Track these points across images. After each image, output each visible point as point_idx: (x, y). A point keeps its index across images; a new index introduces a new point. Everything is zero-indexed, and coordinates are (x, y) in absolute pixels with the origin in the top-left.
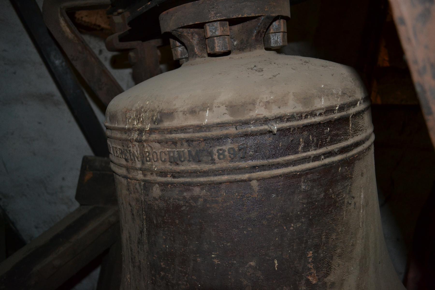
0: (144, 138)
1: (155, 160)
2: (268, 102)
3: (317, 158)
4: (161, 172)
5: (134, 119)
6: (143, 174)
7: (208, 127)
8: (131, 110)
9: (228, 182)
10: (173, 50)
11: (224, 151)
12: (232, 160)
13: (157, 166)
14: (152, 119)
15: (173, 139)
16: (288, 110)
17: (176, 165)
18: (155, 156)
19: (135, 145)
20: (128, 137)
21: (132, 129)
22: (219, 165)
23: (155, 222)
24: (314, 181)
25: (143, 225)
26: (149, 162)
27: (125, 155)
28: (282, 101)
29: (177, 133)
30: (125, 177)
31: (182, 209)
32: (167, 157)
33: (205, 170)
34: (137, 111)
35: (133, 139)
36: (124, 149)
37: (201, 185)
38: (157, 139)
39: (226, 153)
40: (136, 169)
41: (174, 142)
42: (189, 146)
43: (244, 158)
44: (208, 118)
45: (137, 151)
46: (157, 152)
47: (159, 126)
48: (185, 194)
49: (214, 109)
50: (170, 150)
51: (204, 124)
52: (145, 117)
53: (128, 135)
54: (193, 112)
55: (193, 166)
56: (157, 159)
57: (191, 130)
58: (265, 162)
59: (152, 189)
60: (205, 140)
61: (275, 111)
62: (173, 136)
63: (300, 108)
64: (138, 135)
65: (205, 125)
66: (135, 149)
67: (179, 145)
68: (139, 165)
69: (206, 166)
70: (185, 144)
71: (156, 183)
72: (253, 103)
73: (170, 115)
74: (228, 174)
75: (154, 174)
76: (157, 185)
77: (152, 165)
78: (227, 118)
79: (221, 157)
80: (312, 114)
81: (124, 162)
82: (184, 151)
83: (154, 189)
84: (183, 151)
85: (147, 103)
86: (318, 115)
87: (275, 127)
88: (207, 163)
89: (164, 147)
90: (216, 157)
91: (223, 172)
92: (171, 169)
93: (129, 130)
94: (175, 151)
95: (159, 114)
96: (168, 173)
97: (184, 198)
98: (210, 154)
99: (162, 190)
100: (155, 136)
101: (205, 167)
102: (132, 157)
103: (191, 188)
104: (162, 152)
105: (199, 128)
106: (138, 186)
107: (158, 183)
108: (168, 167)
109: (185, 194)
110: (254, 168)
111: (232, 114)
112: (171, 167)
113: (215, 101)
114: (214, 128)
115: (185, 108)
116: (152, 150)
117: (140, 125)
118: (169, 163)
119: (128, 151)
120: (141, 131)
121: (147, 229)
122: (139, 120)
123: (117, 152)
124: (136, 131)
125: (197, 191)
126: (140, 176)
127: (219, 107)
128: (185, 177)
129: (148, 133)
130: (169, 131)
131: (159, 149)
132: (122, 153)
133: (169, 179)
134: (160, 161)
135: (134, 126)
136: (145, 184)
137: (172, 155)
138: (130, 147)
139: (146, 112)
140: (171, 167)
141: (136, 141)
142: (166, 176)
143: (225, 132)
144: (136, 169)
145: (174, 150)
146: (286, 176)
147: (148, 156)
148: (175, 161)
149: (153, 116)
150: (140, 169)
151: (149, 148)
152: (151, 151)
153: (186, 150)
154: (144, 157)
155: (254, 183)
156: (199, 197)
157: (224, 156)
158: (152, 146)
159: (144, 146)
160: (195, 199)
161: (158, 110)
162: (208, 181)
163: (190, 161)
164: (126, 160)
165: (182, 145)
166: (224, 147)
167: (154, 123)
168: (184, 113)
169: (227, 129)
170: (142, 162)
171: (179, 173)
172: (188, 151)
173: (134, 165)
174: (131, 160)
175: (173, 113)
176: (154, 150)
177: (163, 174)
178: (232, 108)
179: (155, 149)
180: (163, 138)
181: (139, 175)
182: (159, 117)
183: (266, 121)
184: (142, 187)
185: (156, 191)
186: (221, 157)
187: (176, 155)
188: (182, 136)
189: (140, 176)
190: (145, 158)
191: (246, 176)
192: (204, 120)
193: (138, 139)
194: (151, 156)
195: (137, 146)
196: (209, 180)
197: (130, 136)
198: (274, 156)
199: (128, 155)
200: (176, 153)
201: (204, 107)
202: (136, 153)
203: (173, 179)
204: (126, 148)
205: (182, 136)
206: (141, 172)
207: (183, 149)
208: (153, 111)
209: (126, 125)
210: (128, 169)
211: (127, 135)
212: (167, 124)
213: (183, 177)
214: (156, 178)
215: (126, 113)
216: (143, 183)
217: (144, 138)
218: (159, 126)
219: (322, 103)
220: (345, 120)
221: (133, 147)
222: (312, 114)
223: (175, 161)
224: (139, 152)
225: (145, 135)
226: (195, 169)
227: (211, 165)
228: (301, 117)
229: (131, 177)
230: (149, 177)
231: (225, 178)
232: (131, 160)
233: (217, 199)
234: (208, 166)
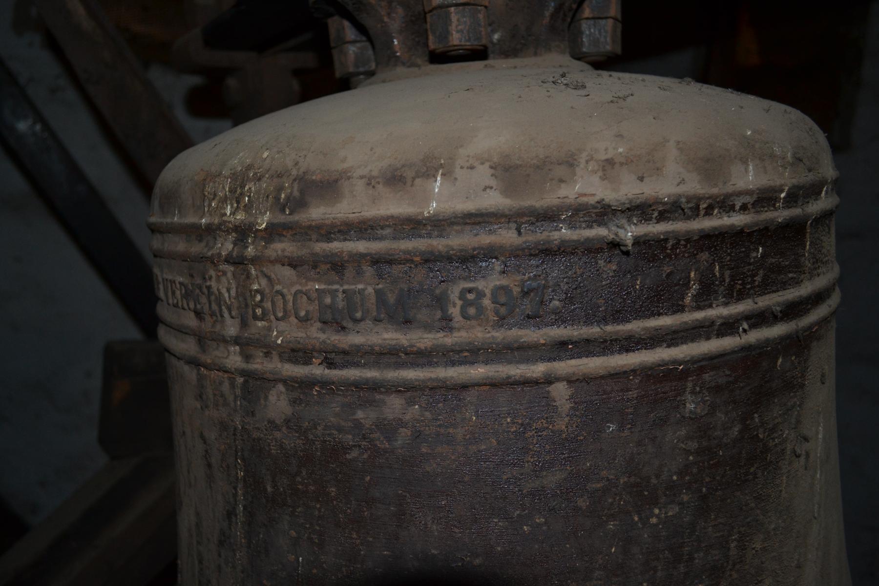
0: (250, 251)
1: (280, 315)
2: (610, 162)
3: (728, 327)
4: (293, 350)
5: (224, 200)
6: (242, 353)
7: (439, 224)
8: (220, 174)
9: (485, 385)
10: (335, 53)
11: (480, 294)
12: (501, 321)
13: (283, 333)
14: (277, 198)
15: (333, 255)
16: (664, 188)
17: (339, 331)
19: (225, 273)
20: (205, 250)
21: (219, 227)
22: (463, 334)
23: (269, 489)
24: (717, 389)
25: (235, 495)
27: (197, 301)
28: (647, 164)
29: (345, 240)
30: (194, 363)
32: (314, 307)
33: (422, 346)
34: (234, 176)
35: (219, 254)
36: (192, 284)
38: (286, 254)
39: (486, 302)
40: (225, 341)
41: (337, 266)
42: (380, 276)
43: (533, 319)
44: (438, 198)
45: (228, 290)
46: (285, 291)
47: (296, 217)
48: (360, 414)
49: (459, 173)
50: (323, 287)
51: (426, 214)
52: (258, 192)
54: (395, 179)
55: (389, 336)
56: (285, 311)
57: (388, 231)
58: (594, 331)
59: (266, 398)
60: (427, 261)
61: (627, 189)
62: (336, 246)
63: (694, 186)
64: (235, 244)
65: (428, 219)
66: (225, 285)
67: (349, 273)
68: (231, 329)
69: (426, 336)
70: (369, 271)
71: (276, 381)
72: (570, 162)
73: (329, 187)
74: (486, 363)
76: (281, 387)
77: (270, 329)
78: (495, 200)
79: (472, 311)
80: (724, 204)
81: (191, 321)
82: (364, 290)
83: (272, 398)
84: (361, 292)
85: (265, 155)
86: (737, 208)
87: (629, 233)
88: (427, 327)
89: (308, 279)
90: (455, 312)
91: (473, 354)
92: (324, 342)
93: (211, 231)
94: (337, 291)
95: (296, 186)
96: (315, 354)
97: (358, 425)
98: (441, 302)
99: (294, 402)
101: (424, 339)
102: (214, 307)
103: (378, 397)
104: (300, 292)
105: (414, 225)
107: (285, 381)
108: (317, 335)
109: (360, 414)
110: (561, 348)
111: (508, 189)
112: (322, 336)
113: (461, 151)
114: (455, 227)
115: (375, 168)
116: (273, 286)
117: (240, 216)
118: (319, 325)
119: (205, 290)
120: (243, 232)
121: (245, 507)
122: (238, 202)
123: (173, 293)
124: (228, 232)
125: (394, 406)
126: (234, 359)
127: (472, 168)
128: (364, 366)
129: (263, 238)
130: (323, 232)
131: (292, 284)
132: (187, 295)
133: (317, 370)
134: (293, 319)
135: (225, 218)
136: (246, 382)
137: (328, 300)
138: (210, 278)
139: (259, 179)
140: (322, 336)
141: (229, 260)
142: (307, 362)
143: (485, 239)
144: (225, 341)
145: (335, 287)
146: (648, 373)
147: (259, 305)
148: (334, 320)
149: (280, 189)
150: (236, 341)
151: (264, 282)
152: (267, 291)
153: (370, 290)
154: (247, 305)
155: (560, 391)
156: (401, 423)
157: (481, 310)
158: (273, 276)
159: (248, 276)
160: (389, 429)
161: (294, 172)
162: (430, 379)
163: (380, 321)
164: (199, 314)
165: (359, 273)
166: (480, 284)
167: (283, 210)
168: (370, 181)
169: (491, 232)
170: (242, 320)
171: (345, 352)
172: (377, 292)
173: (218, 327)
174: (213, 314)
175: (336, 181)
176: (278, 287)
177: (299, 354)
178: (509, 172)
179: (279, 283)
180: (304, 252)
181: (231, 357)
182: (296, 193)
183: (604, 213)
184: (238, 392)
185: (278, 404)
186: (472, 311)
187: (341, 303)
188: (361, 246)
189: (234, 359)
190: (250, 311)
191: (538, 369)
192: (427, 201)
193: (235, 254)
194: (268, 305)
195: (229, 275)
196: (433, 376)
198: (618, 316)
199: (204, 300)
200: (340, 296)
201: (428, 169)
202: (226, 295)
203: (327, 371)
204: (199, 281)
205: (361, 246)
206: (237, 348)
207: (360, 286)
208: (280, 176)
209: (201, 218)
210: (201, 339)
211: (203, 244)
212: (317, 213)
213: (357, 365)
214: (279, 365)
215: (203, 183)
216: (240, 380)
217: (250, 251)
218: (296, 217)
219: (748, 178)
220: (794, 231)
222: (724, 204)
223: (334, 320)
224: (233, 292)
225: (253, 243)
226: (394, 342)
227: (441, 334)
228: (695, 212)
229: (209, 361)
231: (479, 372)
232: (213, 314)
233: (451, 431)
234: (431, 336)
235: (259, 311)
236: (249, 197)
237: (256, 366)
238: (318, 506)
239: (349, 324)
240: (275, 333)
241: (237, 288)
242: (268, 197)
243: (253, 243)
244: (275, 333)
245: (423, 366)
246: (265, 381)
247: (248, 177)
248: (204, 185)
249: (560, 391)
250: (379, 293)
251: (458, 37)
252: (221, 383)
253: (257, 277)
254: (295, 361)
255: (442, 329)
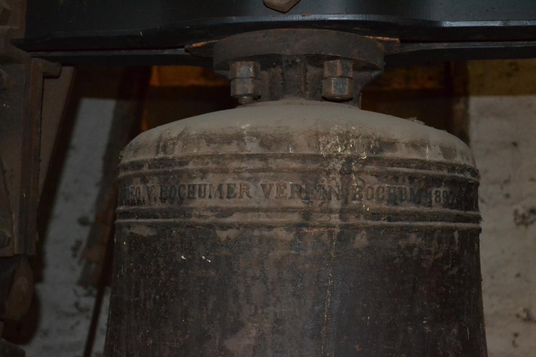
1: (369, 197)
4: (373, 214)
5: (337, 145)
6: (341, 218)
8: (329, 133)
14: (369, 147)
18: (370, 192)
20: (322, 167)
26: (358, 200)
29: (399, 167)
31: (395, 262)
34: (339, 135)
37: (419, 231)
40: (331, 211)
41: (396, 177)
42: (411, 183)
45: (338, 186)
48: (400, 242)
49: (433, 147)
50: (389, 186)
52: (358, 143)
53: (321, 165)
55: (412, 208)
59: (354, 238)
67: (400, 181)
70: (407, 181)
73: (392, 145)
75: (362, 216)
77: (361, 204)
78: (441, 159)
81: (298, 203)
83: (358, 238)
84: (405, 188)
88: (425, 205)
92: (389, 209)
93: (330, 157)
95: (377, 143)
96: (383, 215)
97: (399, 247)
99: (370, 239)
100: (370, 168)
106: (325, 237)
107: (368, 229)
108: (384, 206)
109: (400, 242)
112: (388, 207)
116: (365, 185)
118: (386, 202)
120: (349, 160)
122: (346, 146)
125: (413, 238)
126: (335, 219)
129: (361, 163)
130: (391, 162)
131: (375, 184)
134: (374, 200)
137: (392, 191)
139: (357, 138)
144: (331, 211)
145: (395, 186)
147: (358, 193)
149: (370, 143)
151: (360, 183)
153: (408, 188)
155: (456, 234)
156: (415, 246)
158: (366, 180)
159: (351, 180)
160: (410, 248)
165: (404, 180)
167: (372, 152)
171: (397, 215)
173: (325, 205)
175: (394, 143)
182: (378, 146)
195: (338, 179)
197: (325, 167)
202: (336, 189)
207: (404, 186)
208: (368, 137)
211: (319, 164)
212: (388, 154)
214: (365, 221)
221: (329, 181)
227: (428, 208)
230: (352, 220)
231: (439, 224)
235: (357, 196)
236: (353, 145)
237: (351, 223)
238: (379, 288)
239: (398, 202)
240: (364, 206)
241: (342, 186)
242: (363, 146)
243: (355, 165)
244: (364, 206)
245: (423, 221)
246: (356, 228)
247: (349, 136)
248: (318, 138)
249: (456, 234)
250: (411, 189)
251: (333, 91)
252: (322, 234)
253: (356, 180)
254: (373, 220)
255: (429, 206)
